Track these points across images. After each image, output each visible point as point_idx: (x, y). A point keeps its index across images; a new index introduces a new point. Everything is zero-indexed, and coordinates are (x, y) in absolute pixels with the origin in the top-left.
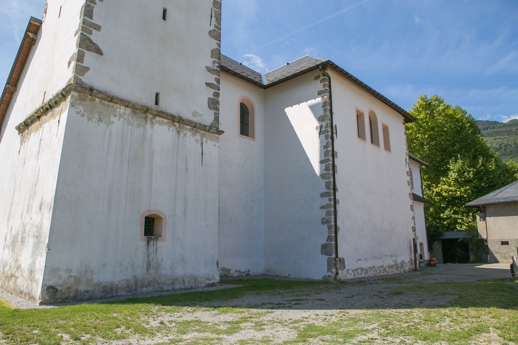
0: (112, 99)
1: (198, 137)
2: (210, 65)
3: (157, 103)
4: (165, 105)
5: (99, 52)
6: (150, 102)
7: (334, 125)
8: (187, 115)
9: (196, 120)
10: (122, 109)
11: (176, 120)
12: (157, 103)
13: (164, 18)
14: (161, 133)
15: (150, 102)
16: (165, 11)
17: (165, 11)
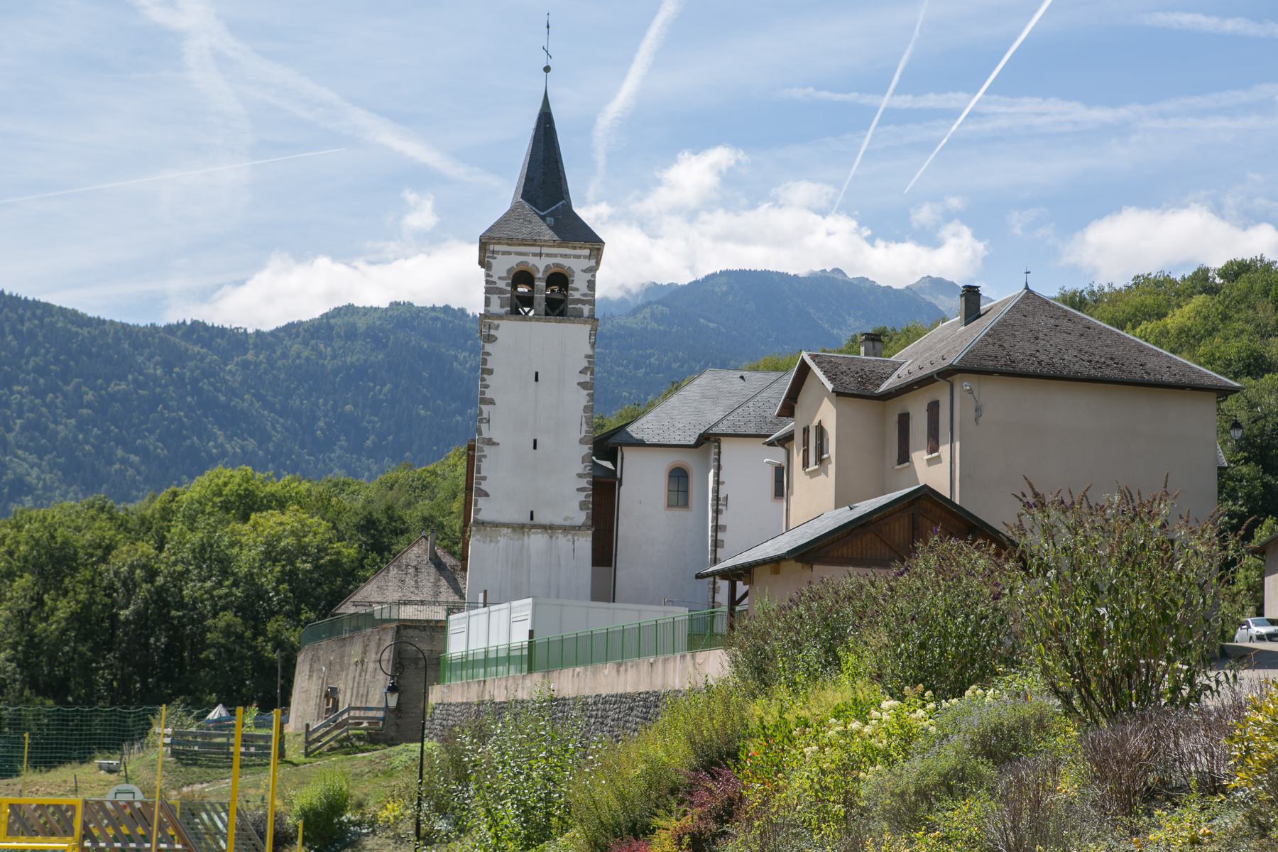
0: (497, 525)
1: (570, 537)
2: (580, 471)
3: (532, 518)
4: (537, 519)
5: (487, 495)
6: (526, 519)
7: (722, 495)
8: (559, 521)
9: (567, 523)
10: (505, 530)
11: (549, 528)
12: (532, 518)
13: (535, 447)
14: (537, 541)
15: (526, 519)
16: (535, 441)
17: (535, 441)
